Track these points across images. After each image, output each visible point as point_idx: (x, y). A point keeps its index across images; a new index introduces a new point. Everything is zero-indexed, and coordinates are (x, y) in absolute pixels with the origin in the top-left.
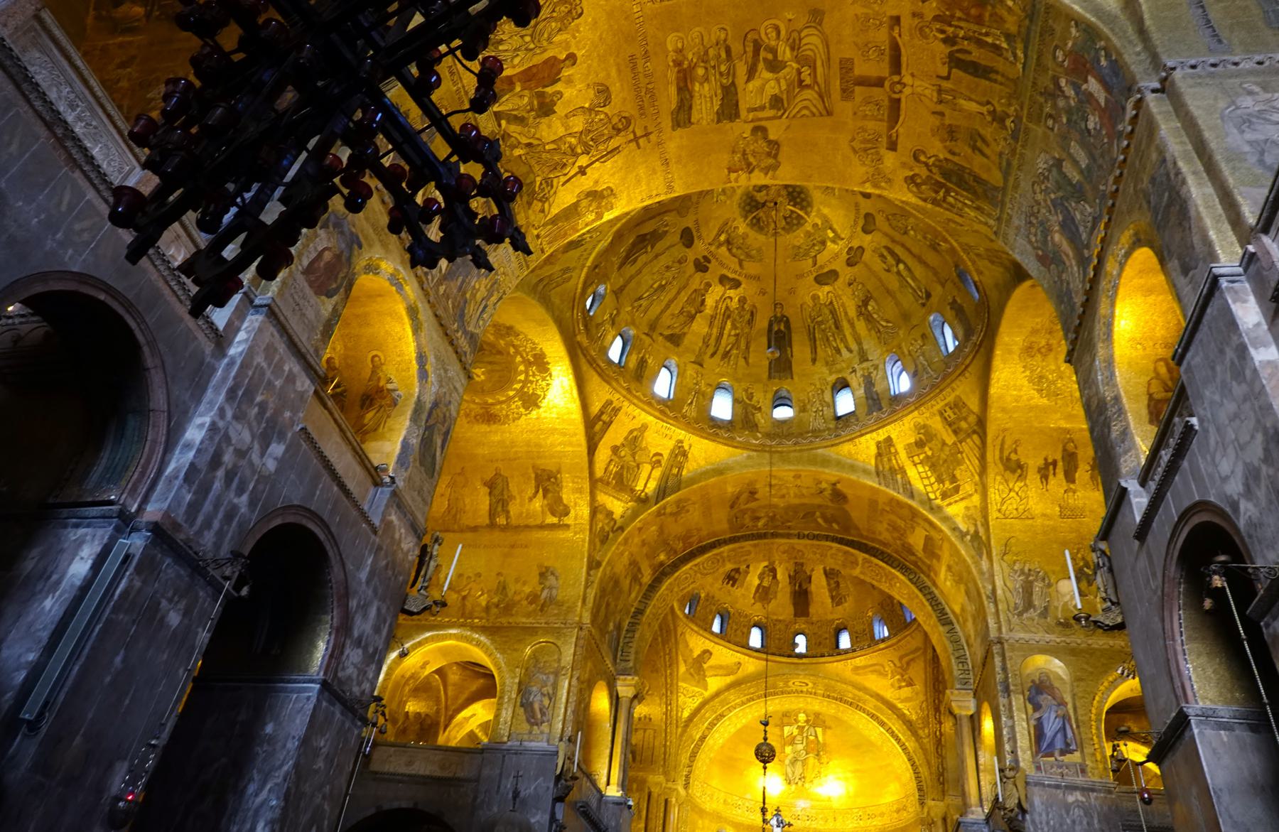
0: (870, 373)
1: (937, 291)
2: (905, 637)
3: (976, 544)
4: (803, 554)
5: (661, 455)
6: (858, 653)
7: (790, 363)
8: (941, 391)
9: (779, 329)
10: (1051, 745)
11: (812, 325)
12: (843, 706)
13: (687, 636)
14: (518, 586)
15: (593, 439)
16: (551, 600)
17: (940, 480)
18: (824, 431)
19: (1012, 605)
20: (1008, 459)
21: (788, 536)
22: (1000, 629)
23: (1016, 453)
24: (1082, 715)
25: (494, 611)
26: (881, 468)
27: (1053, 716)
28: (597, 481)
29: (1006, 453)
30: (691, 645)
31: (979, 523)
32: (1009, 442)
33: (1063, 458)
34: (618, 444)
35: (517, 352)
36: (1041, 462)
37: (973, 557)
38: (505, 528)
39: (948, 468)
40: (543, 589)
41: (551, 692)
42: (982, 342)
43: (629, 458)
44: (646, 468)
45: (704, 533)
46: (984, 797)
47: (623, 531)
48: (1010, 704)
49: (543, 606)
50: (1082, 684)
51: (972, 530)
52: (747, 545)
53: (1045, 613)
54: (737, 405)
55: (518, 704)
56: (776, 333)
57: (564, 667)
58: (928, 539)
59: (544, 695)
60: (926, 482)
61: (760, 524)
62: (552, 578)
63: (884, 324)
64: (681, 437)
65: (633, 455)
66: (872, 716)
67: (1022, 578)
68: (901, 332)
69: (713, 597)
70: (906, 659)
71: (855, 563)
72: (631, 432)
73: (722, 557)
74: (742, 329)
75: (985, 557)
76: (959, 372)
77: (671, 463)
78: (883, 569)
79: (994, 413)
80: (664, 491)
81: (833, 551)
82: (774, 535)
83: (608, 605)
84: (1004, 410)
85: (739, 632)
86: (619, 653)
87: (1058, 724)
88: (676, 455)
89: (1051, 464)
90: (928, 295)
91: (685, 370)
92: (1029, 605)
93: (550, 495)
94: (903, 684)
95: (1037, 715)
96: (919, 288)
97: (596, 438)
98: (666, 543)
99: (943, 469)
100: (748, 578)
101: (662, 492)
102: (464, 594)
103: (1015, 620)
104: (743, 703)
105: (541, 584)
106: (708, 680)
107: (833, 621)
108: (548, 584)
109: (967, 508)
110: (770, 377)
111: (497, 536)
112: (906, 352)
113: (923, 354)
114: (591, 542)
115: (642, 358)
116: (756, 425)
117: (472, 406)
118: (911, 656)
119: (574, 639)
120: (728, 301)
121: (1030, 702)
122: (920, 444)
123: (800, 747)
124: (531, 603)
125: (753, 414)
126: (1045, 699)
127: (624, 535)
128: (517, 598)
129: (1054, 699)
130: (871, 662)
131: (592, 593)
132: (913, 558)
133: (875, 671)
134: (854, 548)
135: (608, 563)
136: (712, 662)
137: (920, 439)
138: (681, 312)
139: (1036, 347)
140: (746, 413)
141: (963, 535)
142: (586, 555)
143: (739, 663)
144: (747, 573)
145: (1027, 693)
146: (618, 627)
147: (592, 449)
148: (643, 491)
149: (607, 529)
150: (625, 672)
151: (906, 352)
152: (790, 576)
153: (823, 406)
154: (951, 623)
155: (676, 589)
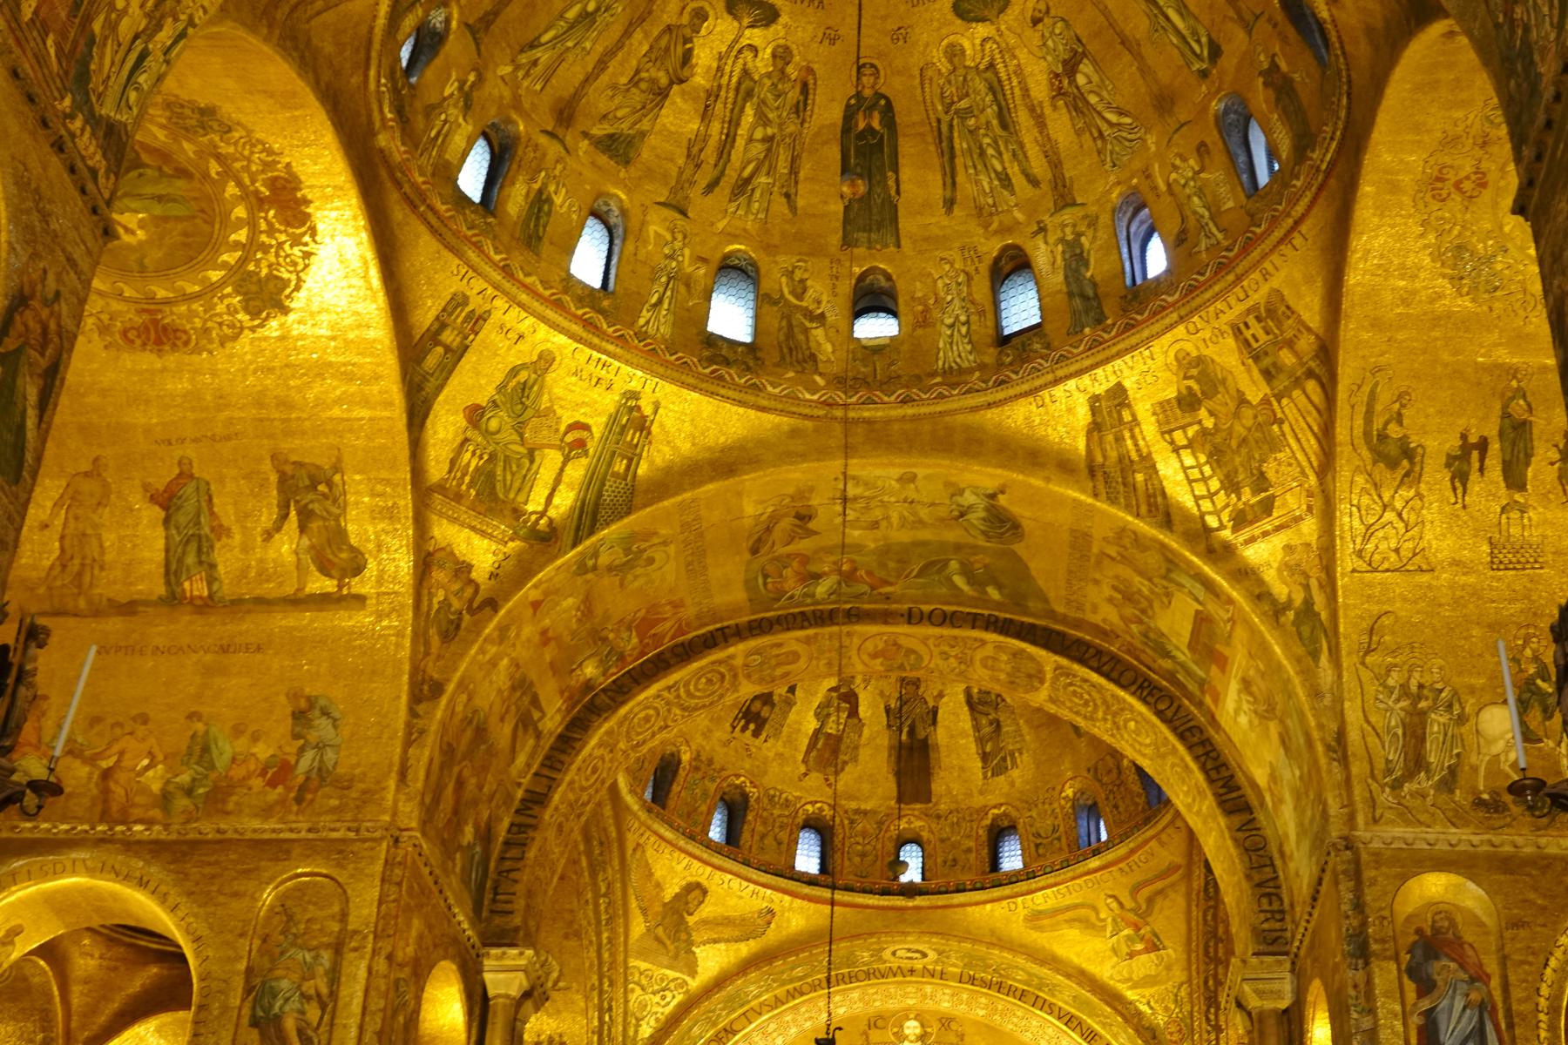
0: (1079, 235)
1: (1236, 41)
2: (1146, 842)
3: (1306, 630)
4: (920, 658)
5: (586, 427)
6: (1041, 881)
7: (895, 209)
8: (1239, 279)
9: (870, 129)
11: (946, 119)
12: (1003, 1002)
13: (650, 852)
14: (242, 744)
15: (420, 388)
16: (322, 775)
17: (1231, 486)
18: (971, 371)
19: (1380, 765)
20: (1383, 437)
21: (885, 617)
22: (1351, 819)
23: (1400, 423)
24: (1520, 1001)
25: (182, 803)
26: (1099, 459)
27: (1459, 1004)
28: (431, 490)
29: (1377, 424)
30: (659, 873)
31: (1314, 583)
32: (1384, 397)
33: (1501, 434)
34: (483, 400)
35: (228, 173)
36: (1453, 443)
37: (1299, 660)
38: (206, 606)
39: (1250, 457)
41: (324, 990)
42: (1332, 163)
43: (508, 435)
44: (551, 460)
45: (690, 612)
47: (496, 611)
48: (1369, 981)
49: (303, 789)
50: (1523, 933)
51: (1298, 598)
52: (791, 639)
53: (1449, 782)
54: (766, 308)
55: (245, 1021)
56: (861, 136)
57: (355, 932)
58: (1202, 621)
60: (1200, 489)
61: (821, 589)
62: (323, 723)
63: (1113, 118)
64: (635, 385)
65: (519, 428)
66: (1069, 1020)
67: (1403, 704)
68: (1151, 140)
69: (710, 762)
70: (1145, 892)
72: (514, 372)
73: (732, 669)
74: (781, 126)
76: (1278, 234)
77: (611, 446)
78: (1099, 689)
79: (1350, 331)
81: (988, 650)
82: (854, 616)
83: (460, 784)
84: (1376, 324)
85: (769, 841)
86: (488, 896)
87: (1468, 1023)
89: (1474, 446)
90: (1215, 52)
91: (643, 223)
92: (1417, 763)
93: (315, 525)
94: (1139, 947)
95: (1425, 1004)
96: (1194, 33)
97: (429, 387)
98: (597, 637)
99: (1238, 460)
100: (792, 716)
101: (589, 517)
102: (105, 764)
103: (1386, 797)
104: (778, 1002)
105: (296, 736)
106: (699, 951)
107: (984, 810)
108: (313, 736)
109: (1288, 548)
110: (847, 242)
111: (185, 624)
112: (1163, 187)
113: (1200, 193)
114: (419, 636)
115: (540, 192)
116: (813, 357)
117: (116, 306)
118: (1159, 885)
119: (378, 867)
120: (748, 55)
121: (1411, 977)
122: (1188, 402)
124: (272, 784)
125: (806, 331)
126: (1444, 969)
127: (496, 620)
128: (238, 772)
129: (1462, 966)
130: (1069, 901)
131: (423, 756)
133: (1078, 920)
134: (1034, 643)
135: (461, 685)
136: (707, 910)
137: (1189, 388)
138: (634, 81)
139: (1452, 177)
140: (790, 326)
141: (1276, 611)
142: (407, 667)
143: (771, 911)
144: (789, 704)
146: (486, 836)
147: (418, 413)
148: (543, 514)
149: (456, 604)
150: (503, 938)
151: (1163, 187)
152: (888, 710)
155: (622, 745)
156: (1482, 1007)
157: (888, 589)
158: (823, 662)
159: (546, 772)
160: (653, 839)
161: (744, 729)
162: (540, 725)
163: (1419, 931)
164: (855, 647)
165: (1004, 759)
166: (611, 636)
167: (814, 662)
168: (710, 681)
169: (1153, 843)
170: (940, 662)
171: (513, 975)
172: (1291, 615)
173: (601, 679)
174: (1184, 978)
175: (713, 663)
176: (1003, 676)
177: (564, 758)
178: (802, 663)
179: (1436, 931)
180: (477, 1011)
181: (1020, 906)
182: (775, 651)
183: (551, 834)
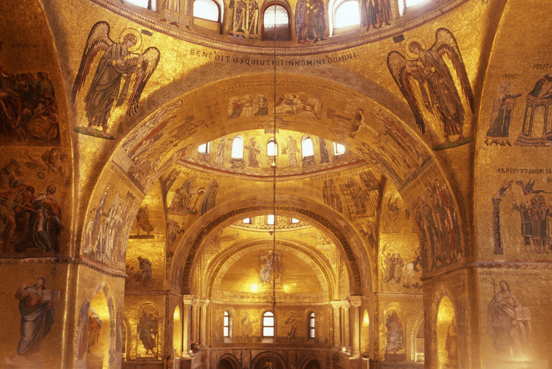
3: (371, 240)
17: (356, 205)
19: (384, 276)
22: (377, 288)
28: (168, 209)
31: (373, 231)
34: (180, 187)
37: (368, 248)
40: (143, 272)
50: (411, 317)
51: (370, 233)
59: (152, 333)
75: (374, 248)
80: (206, 206)
88: (212, 187)
94: (325, 243)
97: (167, 189)
99: (358, 200)
105: (141, 269)
123: (269, 264)
124: (137, 281)
126: (394, 324)
129: (397, 324)
130: (310, 232)
140: (252, 154)
141: (365, 234)
143: (238, 234)
145: (385, 322)
148: (193, 208)
153: (295, 151)
163: (389, 316)
172: (368, 236)
179: (393, 315)
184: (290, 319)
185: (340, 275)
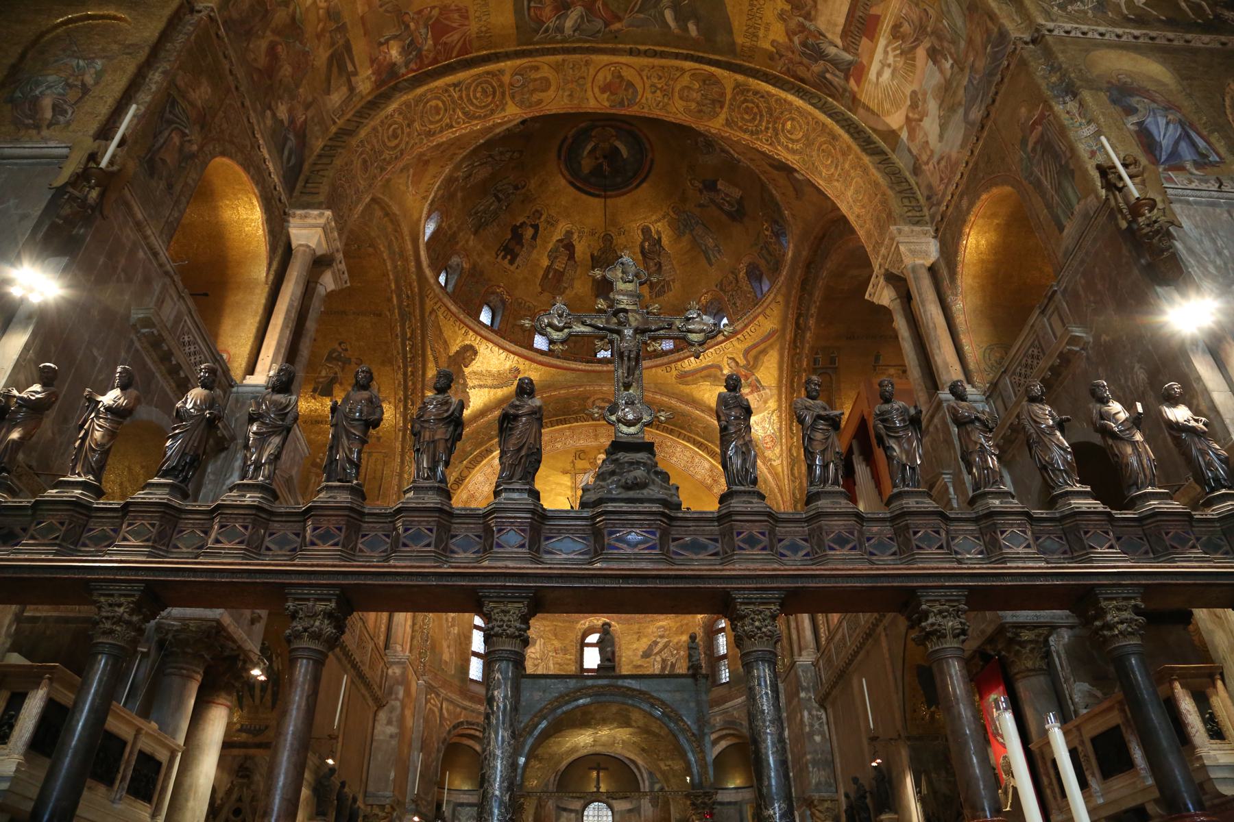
10: (1174, 154)
27: (1162, 122)
45: (474, 27)
46: (972, 366)
70: (754, 352)
71: (718, 102)
73: (502, 85)
81: (686, 80)
86: (300, 185)
87: (1174, 132)
100: (534, 255)
118: (762, 346)
132: (817, 68)
144: (534, 247)
152: (592, 256)
154: (883, 153)
156: (1181, 123)
157: (617, 26)
158: (567, 93)
159: (355, 119)
160: (443, 309)
161: (504, 257)
162: (353, 79)
164: (590, 79)
165: (663, 286)
166: (412, 25)
167: (560, 92)
168: (484, 92)
169: (761, 318)
170: (650, 96)
171: (313, 231)
173: (403, 70)
174: (775, 407)
175: (488, 73)
176: (693, 106)
177: (370, 112)
178: (551, 93)
180: (280, 251)
181: (674, 369)
182: (534, 75)
183: (358, 163)
184: (656, 643)
185: (792, 470)
